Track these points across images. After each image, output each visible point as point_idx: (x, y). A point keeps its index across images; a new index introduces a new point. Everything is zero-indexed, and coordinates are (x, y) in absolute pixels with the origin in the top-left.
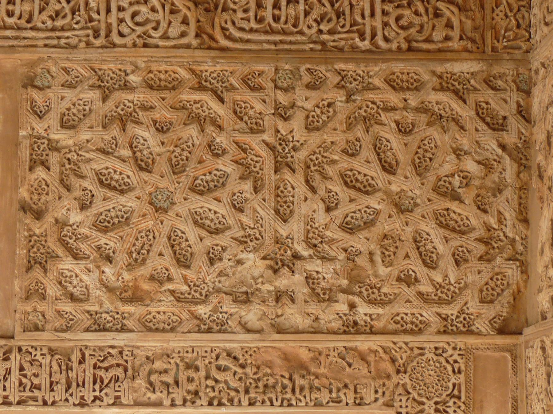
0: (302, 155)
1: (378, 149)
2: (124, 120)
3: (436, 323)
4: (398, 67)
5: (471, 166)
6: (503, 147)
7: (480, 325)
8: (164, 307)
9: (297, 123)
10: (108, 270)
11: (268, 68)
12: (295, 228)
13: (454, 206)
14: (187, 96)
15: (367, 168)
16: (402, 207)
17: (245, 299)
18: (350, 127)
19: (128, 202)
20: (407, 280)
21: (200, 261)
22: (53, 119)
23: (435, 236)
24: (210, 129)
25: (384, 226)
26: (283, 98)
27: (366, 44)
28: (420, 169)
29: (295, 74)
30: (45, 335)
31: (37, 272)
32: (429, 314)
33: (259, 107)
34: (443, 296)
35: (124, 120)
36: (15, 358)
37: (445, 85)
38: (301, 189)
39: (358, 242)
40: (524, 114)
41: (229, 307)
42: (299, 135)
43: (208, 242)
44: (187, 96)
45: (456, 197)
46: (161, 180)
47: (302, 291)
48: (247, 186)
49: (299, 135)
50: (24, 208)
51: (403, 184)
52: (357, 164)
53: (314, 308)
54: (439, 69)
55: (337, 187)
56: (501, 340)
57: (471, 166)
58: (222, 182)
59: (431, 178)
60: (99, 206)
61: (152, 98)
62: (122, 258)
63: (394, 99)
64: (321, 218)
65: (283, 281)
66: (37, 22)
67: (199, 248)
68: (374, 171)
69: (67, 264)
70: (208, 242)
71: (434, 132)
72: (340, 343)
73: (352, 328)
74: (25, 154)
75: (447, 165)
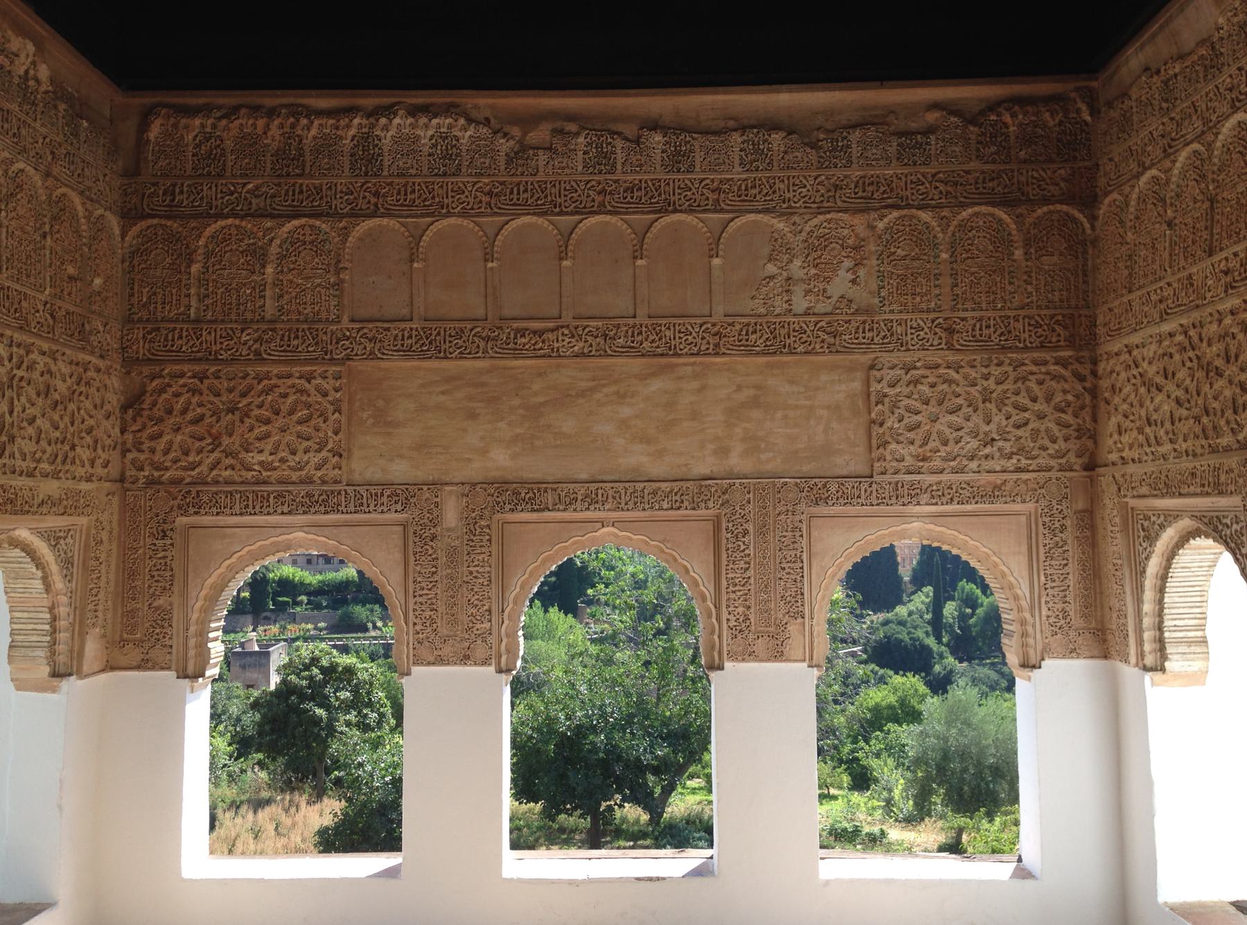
0: (994, 395)
1: (1028, 390)
2: (916, 382)
3: (1057, 467)
4: (1036, 355)
6: (1084, 388)
7: (1076, 467)
8: (937, 463)
10: (911, 447)
11: (978, 358)
12: (993, 426)
13: (1063, 415)
14: (942, 371)
15: (1023, 400)
16: (1041, 417)
17: (972, 458)
18: (1015, 382)
19: (919, 418)
20: (1044, 449)
21: (951, 443)
22: (884, 383)
23: (1056, 429)
24: (954, 386)
25: (1031, 426)
26: (985, 371)
27: (1021, 345)
28: (1048, 399)
29: (990, 359)
31: (881, 450)
32: (1053, 463)
34: (1060, 455)
35: (916, 382)
36: (874, 486)
37: (1057, 362)
38: (994, 410)
39: (1019, 432)
40: (1094, 373)
42: (993, 387)
43: (954, 435)
45: (1064, 412)
46: (932, 408)
47: (997, 455)
49: (993, 387)
50: (874, 422)
52: (1019, 399)
53: (1003, 462)
54: (1055, 355)
55: (1010, 409)
56: (1085, 473)
57: (1070, 397)
58: (959, 408)
59: (1053, 404)
60: (906, 421)
61: (927, 372)
62: (918, 443)
63: (1034, 369)
64: (1004, 423)
65: (987, 450)
67: (951, 437)
68: (1027, 402)
69: (893, 446)
70: (954, 435)
71: (1053, 383)
72: (1015, 476)
73: (1019, 470)
74: (873, 399)
75: (1058, 398)
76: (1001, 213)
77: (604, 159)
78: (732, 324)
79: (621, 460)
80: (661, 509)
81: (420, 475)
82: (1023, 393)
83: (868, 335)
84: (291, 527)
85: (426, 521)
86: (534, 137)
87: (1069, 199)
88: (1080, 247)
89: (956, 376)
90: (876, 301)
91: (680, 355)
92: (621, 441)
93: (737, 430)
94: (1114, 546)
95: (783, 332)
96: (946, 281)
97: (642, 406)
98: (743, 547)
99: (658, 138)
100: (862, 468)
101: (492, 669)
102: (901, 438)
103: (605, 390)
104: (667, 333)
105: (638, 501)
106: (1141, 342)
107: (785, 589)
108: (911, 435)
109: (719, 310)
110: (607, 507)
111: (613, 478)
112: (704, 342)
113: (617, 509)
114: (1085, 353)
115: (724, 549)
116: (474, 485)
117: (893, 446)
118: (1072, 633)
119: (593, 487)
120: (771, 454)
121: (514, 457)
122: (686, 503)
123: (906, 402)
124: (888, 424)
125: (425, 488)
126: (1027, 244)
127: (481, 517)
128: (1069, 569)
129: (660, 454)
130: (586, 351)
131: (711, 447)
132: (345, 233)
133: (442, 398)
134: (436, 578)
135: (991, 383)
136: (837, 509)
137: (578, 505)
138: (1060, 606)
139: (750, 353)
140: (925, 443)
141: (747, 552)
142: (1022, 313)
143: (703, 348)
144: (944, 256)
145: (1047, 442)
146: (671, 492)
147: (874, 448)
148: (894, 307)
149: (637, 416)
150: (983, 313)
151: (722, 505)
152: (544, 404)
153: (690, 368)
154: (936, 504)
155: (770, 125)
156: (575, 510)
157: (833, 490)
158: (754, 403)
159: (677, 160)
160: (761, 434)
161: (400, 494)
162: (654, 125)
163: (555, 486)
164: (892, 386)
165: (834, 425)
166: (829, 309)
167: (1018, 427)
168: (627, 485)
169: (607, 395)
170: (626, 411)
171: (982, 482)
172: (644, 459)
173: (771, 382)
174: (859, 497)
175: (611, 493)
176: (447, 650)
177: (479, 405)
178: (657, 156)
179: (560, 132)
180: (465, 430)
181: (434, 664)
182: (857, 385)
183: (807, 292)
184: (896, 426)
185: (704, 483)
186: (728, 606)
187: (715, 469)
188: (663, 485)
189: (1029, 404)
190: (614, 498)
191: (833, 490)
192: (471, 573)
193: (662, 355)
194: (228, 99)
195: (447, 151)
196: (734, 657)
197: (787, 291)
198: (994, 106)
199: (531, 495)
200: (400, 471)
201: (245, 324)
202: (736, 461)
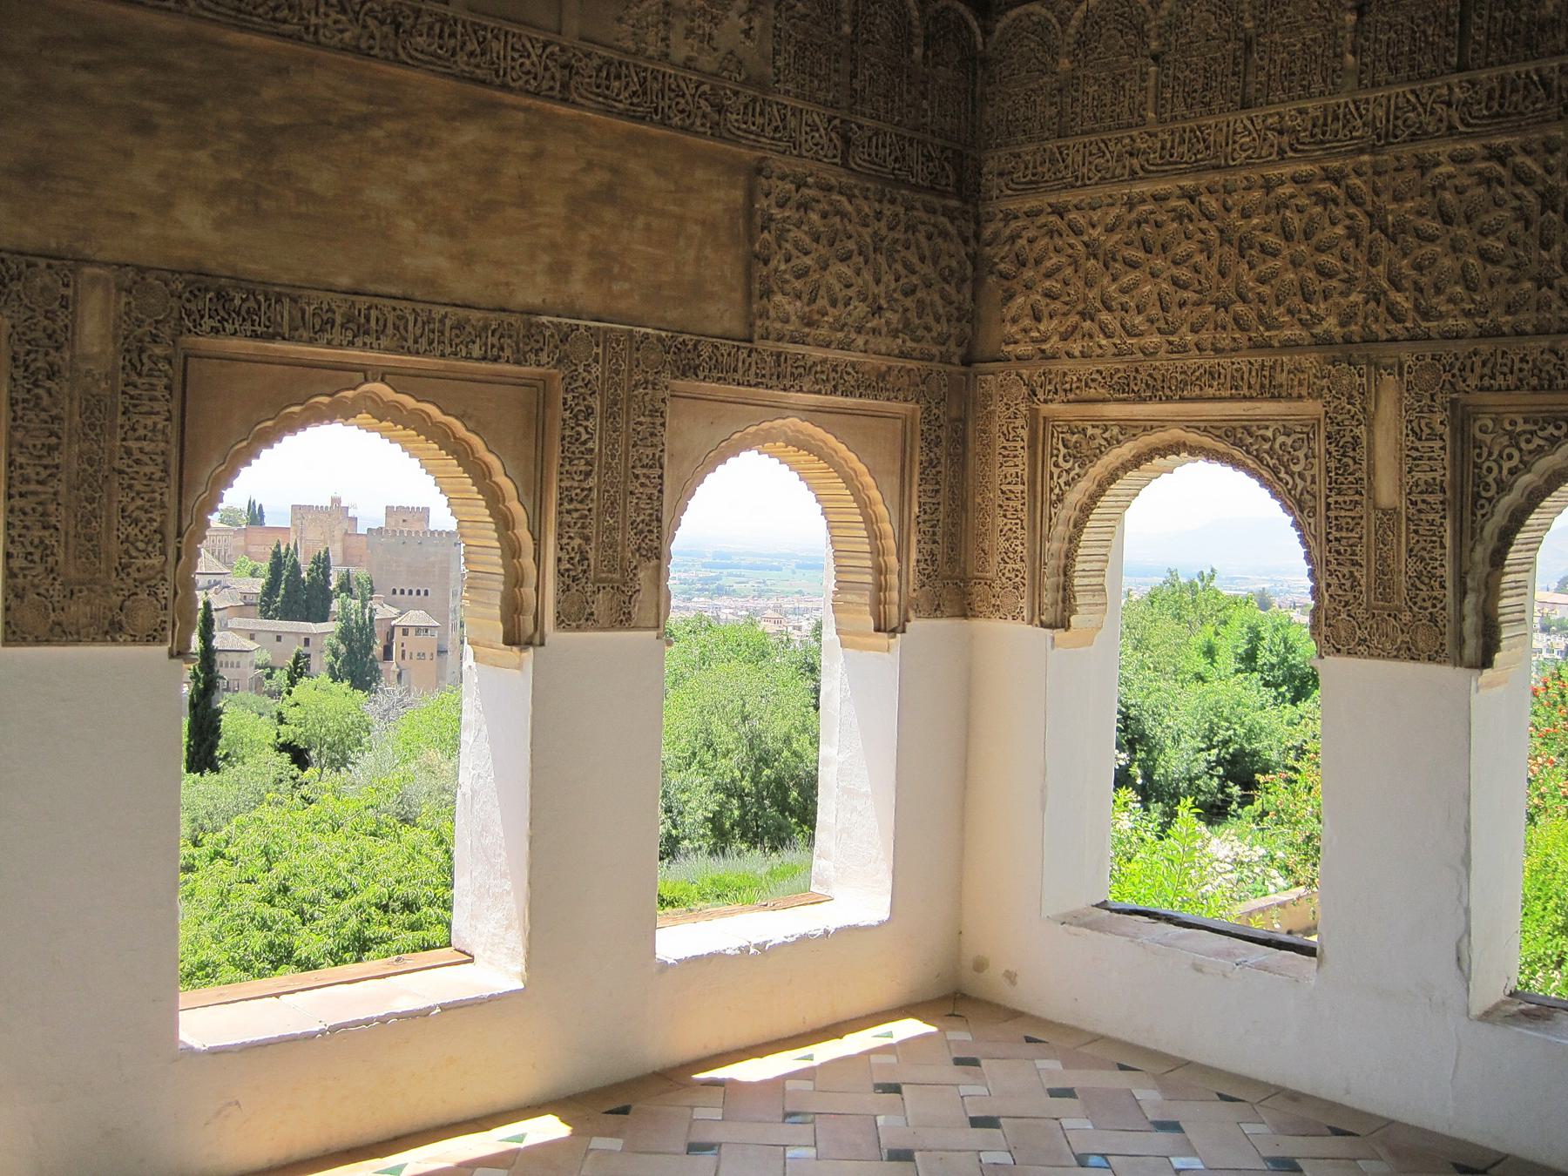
1: (918, 247)
2: (804, 206)
5: (954, 264)
8: (823, 332)
9: (883, 223)
10: (798, 304)
12: (882, 287)
13: (947, 287)
17: (859, 331)
19: (808, 261)
20: (929, 329)
21: (840, 305)
22: (772, 197)
25: (919, 294)
29: (883, 191)
30: (770, 343)
32: (935, 350)
33: (867, 210)
34: (942, 340)
36: (754, 355)
37: (947, 212)
38: (885, 267)
39: (909, 302)
40: (977, 236)
41: (853, 335)
42: (884, 232)
44: (836, 197)
46: (823, 249)
47: (884, 330)
48: (861, 259)
49: (884, 232)
50: (756, 256)
51: (926, 269)
53: (889, 340)
55: (899, 266)
56: (963, 369)
57: (954, 264)
62: (806, 297)
63: (924, 216)
64: (893, 285)
66: (768, 131)
67: (840, 296)
68: (915, 260)
69: (778, 298)
71: (940, 241)
72: (900, 363)
73: (903, 355)
74: (758, 220)
75: (943, 263)
78: (588, 55)
79: (406, 261)
80: (469, 357)
81: (30, 235)
82: (913, 248)
83: (759, 121)
85: (39, 334)
89: (849, 208)
90: (770, 70)
91: (511, 90)
92: (408, 225)
93: (583, 236)
95: (656, 86)
96: (844, 65)
97: (445, 166)
98: (584, 437)
100: (737, 327)
101: (165, 649)
102: (787, 287)
103: (389, 126)
104: (494, 44)
105: (433, 337)
107: (638, 510)
108: (798, 284)
109: (573, 25)
110: (384, 342)
111: (393, 290)
112: (548, 75)
113: (401, 349)
114: (969, 208)
115: (558, 438)
116: (141, 270)
117: (778, 298)
118: (938, 584)
119: (362, 302)
120: (627, 286)
121: (220, 224)
122: (508, 352)
123: (794, 233)
124: (773, 264)
125: (42, 263)
126: (926, 46)
127: (155, 339)
128: (940, 498)
129: (468, 259)
130: (363, 45)
131: (546, 259)
133: (83, 78)
134: (57, 458)
135: (882, 227)
136: (708, 386)
137: (336, 335)
138: (928, 547)
139: (608, 111)
140: (812, 301)
141: (590, 445)
142: (918, 136)
143: (545, 85)
144: (847, 29)
145: (932, 323)
146: (485, 328)
147: (755, 298)
148: (790, 86)
149: (436, 184)
150: (881, 125)
151: (559, 361)
152: (282, 130)
153: (521, 116)
154: (819, 392)
156: (329, 344)
157: (705, 356)
158: (607, 195)
160: (614, 248)
163: (298, 292)
164: (781, 206)
165: (708, 252)
166: (714, 67)
167: (906, 294)
168: (419, 307)
169: (389, 136)
170: (419, 172)
171: (867, 368)
172: (443, 263)
173: (633, 165)
174: (735, 370)
175: (391, 318)
176: (78, 611)
177: (159, 106)
180: (127, 154)
181: (48, 642)
182: (738, 195)
183: (690, 32)
184: (783, 267)
185: (534, 319)
186: (560, 536)
187: (549, 297)
188: (475, 315)
189: (918, 266)
190: (396, 328)
191: (705, 356)
192: (129, 452)
193: (483, 82)
196: (562, 622)
197: (666, 23)
199: (252, 304)
202: (577, 287)
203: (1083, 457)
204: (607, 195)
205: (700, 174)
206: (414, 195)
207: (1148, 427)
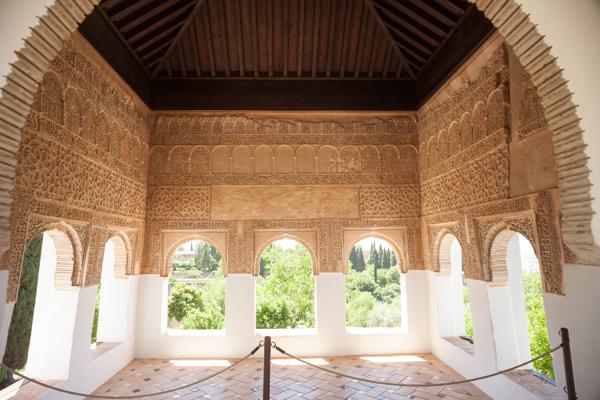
76: (394, 147)
77: (285, 129)
84: (193, 233)
86: (265, 123)
87: (412, 143)
88: (415, 156)
94: (425, 238)
99: (300, 124)
106: (431, 182)
129: (301, 212)
132: (211, 149)
155: (332, 121)
158: (327, 198)
159: (305, 130)
161: (226, 224)
162: (299, 120)
170: (291, 200)
178: (300, 128)
179: (272, 122)
194: (179, 112)
195: (241, 127)
196: (321, 271)
198: (391, 118)
200: (225, 217)
201: (182, 174)
202: (322, 214)
203: (435, 235)
204: (327, 198)
205: (347, 191)
206: (290, 204)
207: (441, 228)
